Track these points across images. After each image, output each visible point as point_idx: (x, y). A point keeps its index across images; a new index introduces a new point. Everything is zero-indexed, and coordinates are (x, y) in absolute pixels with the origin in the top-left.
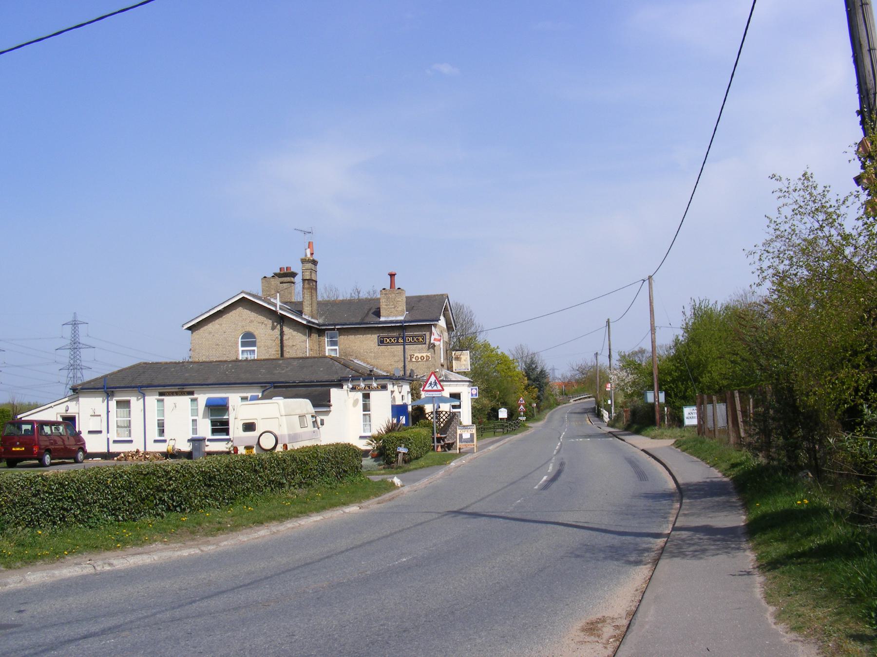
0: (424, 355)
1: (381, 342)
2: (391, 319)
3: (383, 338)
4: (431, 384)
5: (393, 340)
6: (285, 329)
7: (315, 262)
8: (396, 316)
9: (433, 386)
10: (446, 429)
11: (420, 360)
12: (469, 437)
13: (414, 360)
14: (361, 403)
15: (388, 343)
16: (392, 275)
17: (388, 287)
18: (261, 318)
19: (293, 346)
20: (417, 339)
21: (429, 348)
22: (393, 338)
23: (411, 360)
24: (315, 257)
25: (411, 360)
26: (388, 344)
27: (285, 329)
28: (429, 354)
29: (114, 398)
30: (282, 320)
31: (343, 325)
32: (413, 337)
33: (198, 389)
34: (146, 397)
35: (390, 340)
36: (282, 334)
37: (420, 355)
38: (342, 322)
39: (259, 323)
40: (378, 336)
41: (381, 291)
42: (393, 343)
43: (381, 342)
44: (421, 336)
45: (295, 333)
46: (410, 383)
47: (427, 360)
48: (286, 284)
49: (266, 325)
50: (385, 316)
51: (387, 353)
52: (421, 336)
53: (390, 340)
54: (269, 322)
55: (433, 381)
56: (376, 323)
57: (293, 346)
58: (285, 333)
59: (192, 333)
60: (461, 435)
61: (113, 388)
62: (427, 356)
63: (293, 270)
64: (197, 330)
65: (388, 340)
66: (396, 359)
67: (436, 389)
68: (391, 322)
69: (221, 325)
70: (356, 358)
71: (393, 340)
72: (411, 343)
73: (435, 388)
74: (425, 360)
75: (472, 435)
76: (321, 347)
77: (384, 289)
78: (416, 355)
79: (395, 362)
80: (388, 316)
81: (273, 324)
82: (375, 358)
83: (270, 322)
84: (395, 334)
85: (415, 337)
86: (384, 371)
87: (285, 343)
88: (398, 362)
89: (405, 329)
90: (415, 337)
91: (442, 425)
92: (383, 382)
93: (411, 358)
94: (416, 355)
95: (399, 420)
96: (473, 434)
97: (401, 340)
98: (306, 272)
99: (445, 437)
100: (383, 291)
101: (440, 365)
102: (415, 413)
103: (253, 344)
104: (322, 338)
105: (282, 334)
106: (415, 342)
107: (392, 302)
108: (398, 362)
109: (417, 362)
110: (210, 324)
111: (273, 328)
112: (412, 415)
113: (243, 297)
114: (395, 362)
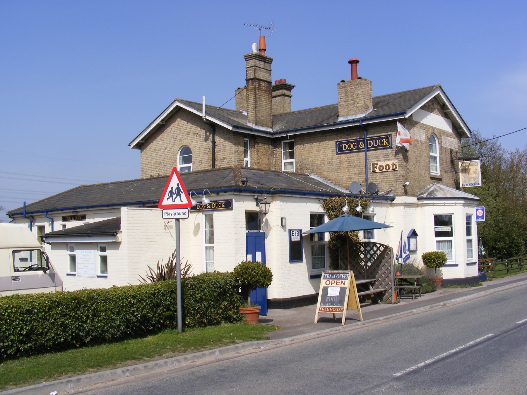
0: (390, 163)
1: (340, 150)
2: (350, 118)
3: (341, 144)
4: (171, 192)
5: (352, 146)
6: (218, 139)
7: (267, 61)
8: (356, 114)
9: (174, 196)
10: (375, 269)
11: (384, 170)
12: (337, 294)
13: (377, 170)
14: (203, 229)
15: (347, 150)
16: (354, 63)
17: (348, 78)
18: (196, 129)
19: (224, 158)
20: (381, 143)
21: (397, 154)
22: (352, 143)
23: (374, 171)
24: (267, 54)
25: (374, 171)
26: (348, 152)
27: (218, 139)
28: (395, 162)
29: (36, 224)
30: (213, 128)
31: (296, 131)
32: (375, 139)
33: (91, 213)
34: (55, 223)
35: (350, 146)
36: (214, 143)
37: (384, 164)
38: (294, 127)
39: (194, 134)
40: (337, 142)
41: (339, 84)
42: (352, 149)
43: (340, 150)
44: (385, 138)
45: (226, 143)
46: (325, 200)
47: (394, 170)
48: (279, 98)
49: (200, 136)
50: (343, 116)
51: (346, 164)
52: (385, 138)
53: (350, 146)
54: (202, 132)
55: (175, 187)
56: (330, 125)
57: (224, 158)
58: (217, 144)
59: (141, 152)
60: (325, 290)
61: (32, 213)
62: (393, 165)
63: (288, 82)
64: (145, 148)
65: (347, 147)
66: (357, 170)
67: (179, 203)
68: (354, 121)
69: (163, 140)
70: (313, 172)
71: (352, 146)
72: (373, 149)
73: (178, 201)
74: (391, 170)
75: (343, 290)
76: (276, 159)
77: (343, 81)
78: (380, 164)
79: (355, 174)
80: (348, 115)
81: (206, 135)
82: (333, 170)
83: (204, 131)
84: (355, 138)
85: (379, 139)
86: (344, 187)
87: (217, 156)
88: (359, 174)
89: (367, 131)
90: (379, 139)
91: (369, 264)
92: (223, 197)
93: (375, 168)
94: (380, 164)
95: (254, 257)
96: (345, 288)
97: (362, 146)
98: (250, 70)
99: (375, 281)
100: (341, 84)
101: (429, 179)
102: (334, 245)
103: (190, 161)
104: (278, 150)
105: (214, 143)
106: (379, 146)
107: (352, 96)
108: (359, 174)
109: (381, 172)
110: (155, 141)
111: (206, 139)
112: (330, 248)
113: (177, 107)
114: (355, 174)
